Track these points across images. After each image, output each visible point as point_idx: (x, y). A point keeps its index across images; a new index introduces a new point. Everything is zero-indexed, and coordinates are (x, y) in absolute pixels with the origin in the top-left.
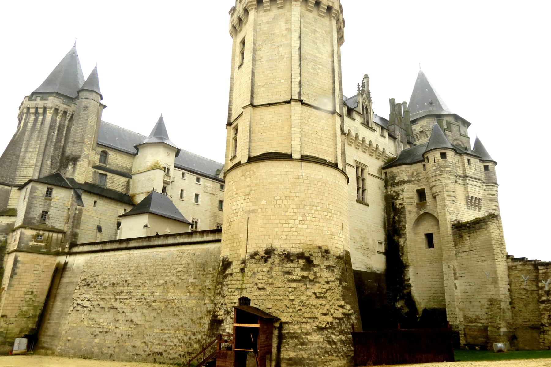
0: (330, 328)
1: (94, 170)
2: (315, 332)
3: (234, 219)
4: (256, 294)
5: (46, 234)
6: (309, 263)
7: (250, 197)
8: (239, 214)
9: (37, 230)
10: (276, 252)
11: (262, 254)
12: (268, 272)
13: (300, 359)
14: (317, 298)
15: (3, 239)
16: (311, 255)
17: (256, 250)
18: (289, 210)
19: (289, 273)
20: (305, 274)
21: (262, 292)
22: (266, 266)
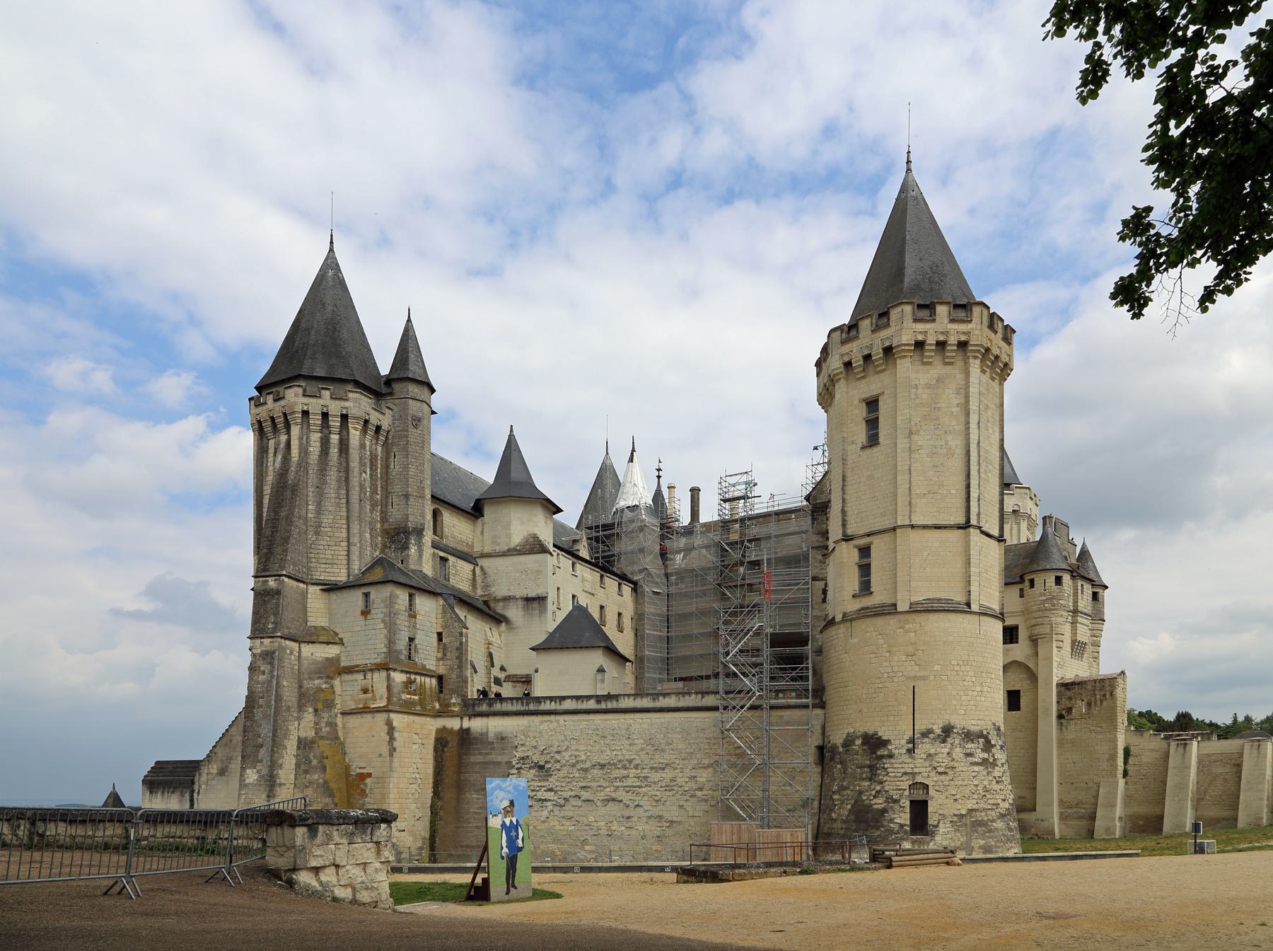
0: (1008, 814)
1: (433, 550)
2: (998, 818)
3: (887, 685)
4: (935, 779)
5: (418, 678)
6: (988, 746)
7: (914, 658)
8: (895, 679)
9: (407, 672)
10: (955, 731)
11: (938, 731)
12: (948, 753)
13: (989, 847)
14: (998, 782)
15: (324, 686)
16: (988, 733)
17: (930, 726)
18: (968, 678)
19: (968, 755)
20: (986, 756)
21: (943, 777)
22: (945, 747)
